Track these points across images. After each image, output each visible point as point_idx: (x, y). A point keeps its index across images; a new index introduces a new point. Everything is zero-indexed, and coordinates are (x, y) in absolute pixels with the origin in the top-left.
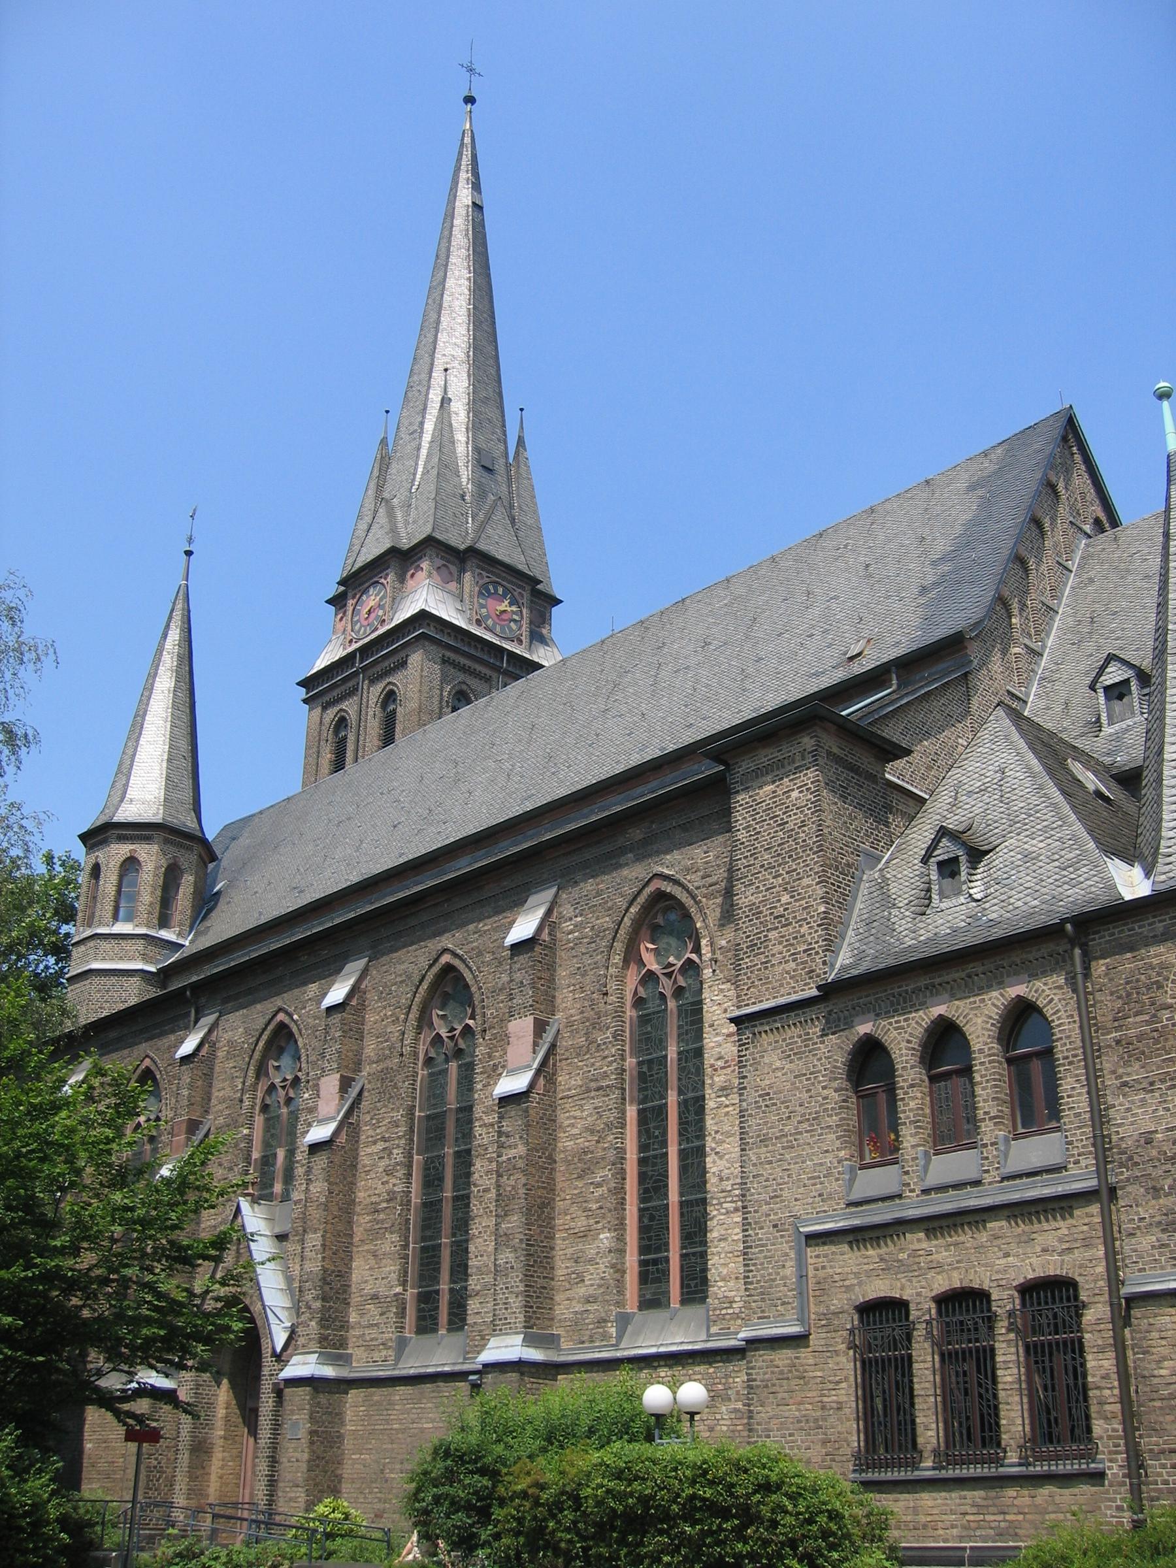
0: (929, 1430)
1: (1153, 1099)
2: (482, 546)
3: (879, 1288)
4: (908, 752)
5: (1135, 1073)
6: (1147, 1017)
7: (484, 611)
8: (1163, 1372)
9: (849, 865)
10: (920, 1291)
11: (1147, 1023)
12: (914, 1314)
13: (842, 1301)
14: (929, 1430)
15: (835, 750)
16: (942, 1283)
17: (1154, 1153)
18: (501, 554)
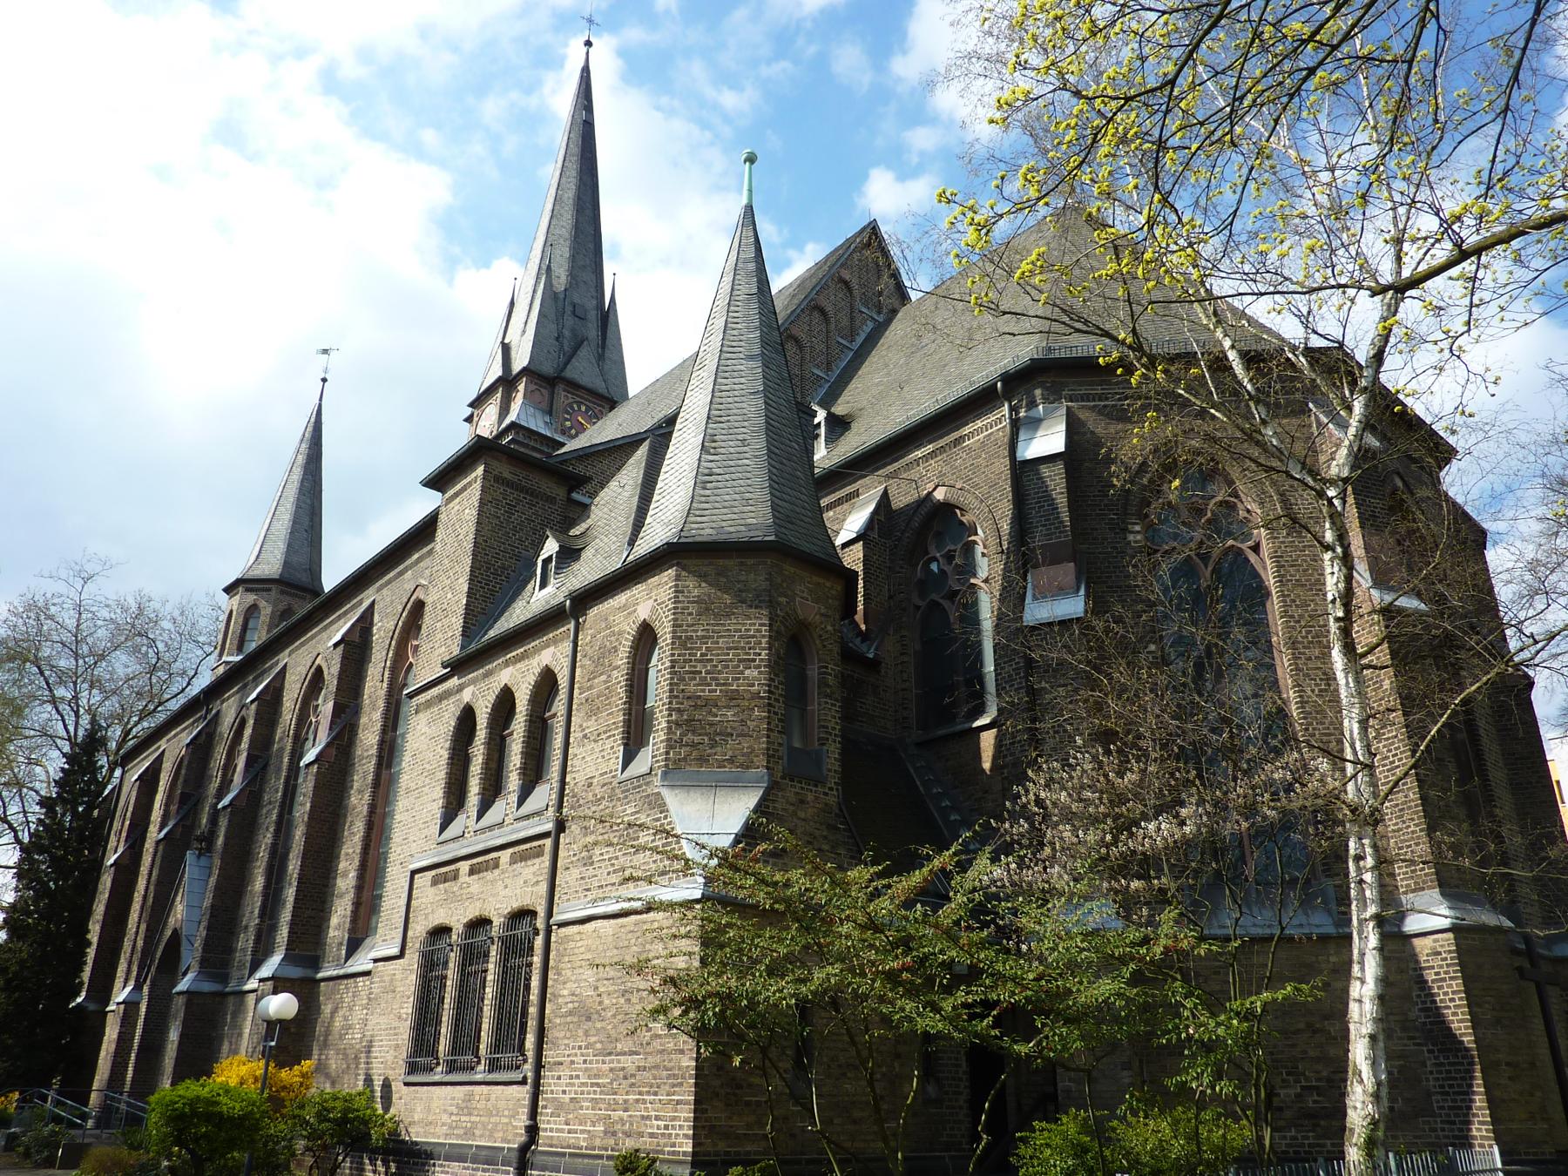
0: (443, 1046)
1: (597, 747)
2: (569, 373)
3: (439, 918)
4: (590, 479)
5: (592, 725)
6: (603, 678)
7: (568, 424)
8: (565, 992)
9: (503, 568)
10: (457, 920)
11: (606, 682)
12: (454, 937)
13: (419, 929)
14: (443, 1046)
15: (506, 475)
16: (472, 913)
17: (590, 797)
18: (585, 380)
